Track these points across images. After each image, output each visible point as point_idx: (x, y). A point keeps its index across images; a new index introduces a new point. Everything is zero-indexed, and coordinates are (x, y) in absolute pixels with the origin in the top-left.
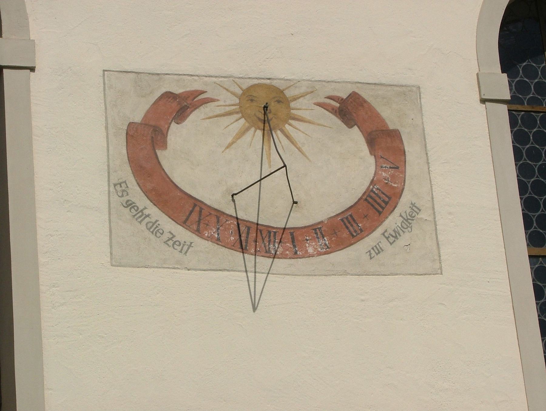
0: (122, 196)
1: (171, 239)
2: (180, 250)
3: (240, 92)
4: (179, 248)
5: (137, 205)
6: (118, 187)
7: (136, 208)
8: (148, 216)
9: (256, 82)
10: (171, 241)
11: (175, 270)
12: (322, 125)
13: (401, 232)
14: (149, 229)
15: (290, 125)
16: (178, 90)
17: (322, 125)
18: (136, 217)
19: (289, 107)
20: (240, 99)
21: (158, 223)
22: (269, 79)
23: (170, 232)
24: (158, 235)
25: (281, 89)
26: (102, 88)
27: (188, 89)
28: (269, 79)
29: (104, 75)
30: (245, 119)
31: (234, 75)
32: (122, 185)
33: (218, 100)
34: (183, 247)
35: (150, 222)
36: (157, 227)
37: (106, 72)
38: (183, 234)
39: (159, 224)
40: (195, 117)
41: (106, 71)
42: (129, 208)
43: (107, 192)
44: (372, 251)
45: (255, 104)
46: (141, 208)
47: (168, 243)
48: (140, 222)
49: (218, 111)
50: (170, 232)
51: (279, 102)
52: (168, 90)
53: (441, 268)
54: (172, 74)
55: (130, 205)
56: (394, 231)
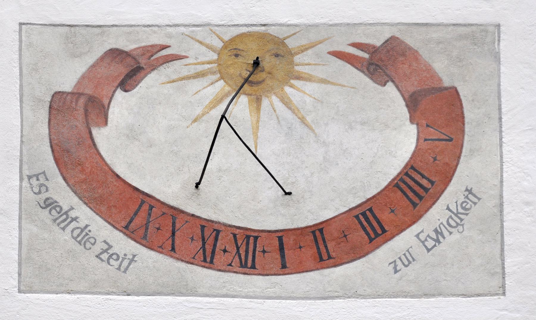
0: (40, 192)
1: (105, 251)
2: (117, 267)
3: (219, 44)
4: (116, 264)
5: (61, 204)
6: (34, 181)
7: (58, 209)
8: (75, 219)
9: (244, 30)
10: (106, 253)
11: (108, 297)
12: (340, 85)
13: (446, 233)
14: (75, 239)
15: (292, 86)
16: (128, 46)
17: (340, 85)
18: (58, 221)
19: (292, 63)
20: (219, 54)
21: (89, 228)
22: (264, 25)
23: (105, 242)
24: (88, 245)
25: (281, 37)
26: (17, 47)
27: (143, 44)
28: (264, 25)
29: (20, 30)
30: (225, 81)
31: (213, 22)
32: (40, 177)
33: (187, 57)
34: (122, 262)
35: (78, 228)
36: (87, 234)
37: (23, 26)
38: (123, 244)
39: (90, 231)
40: (151, 83)
41: (24, 24)
42: (49, 209)
43: (18, 188)
44: (399, 263)
45: (240, 60)
46: (65, 208)
47: (102, 256)
48: (63, 229)
49: (185, 72)
50: (105, 242)
51: (277, 55)
52: (114, 46)
53: (503, 286)
54: (125, 26)
55: (49, 204)
56: (436, 231)
